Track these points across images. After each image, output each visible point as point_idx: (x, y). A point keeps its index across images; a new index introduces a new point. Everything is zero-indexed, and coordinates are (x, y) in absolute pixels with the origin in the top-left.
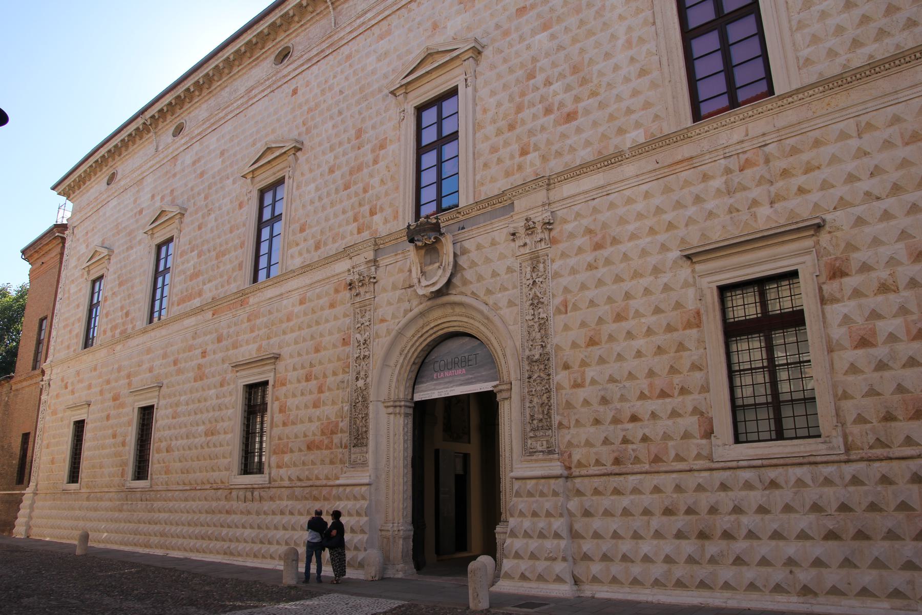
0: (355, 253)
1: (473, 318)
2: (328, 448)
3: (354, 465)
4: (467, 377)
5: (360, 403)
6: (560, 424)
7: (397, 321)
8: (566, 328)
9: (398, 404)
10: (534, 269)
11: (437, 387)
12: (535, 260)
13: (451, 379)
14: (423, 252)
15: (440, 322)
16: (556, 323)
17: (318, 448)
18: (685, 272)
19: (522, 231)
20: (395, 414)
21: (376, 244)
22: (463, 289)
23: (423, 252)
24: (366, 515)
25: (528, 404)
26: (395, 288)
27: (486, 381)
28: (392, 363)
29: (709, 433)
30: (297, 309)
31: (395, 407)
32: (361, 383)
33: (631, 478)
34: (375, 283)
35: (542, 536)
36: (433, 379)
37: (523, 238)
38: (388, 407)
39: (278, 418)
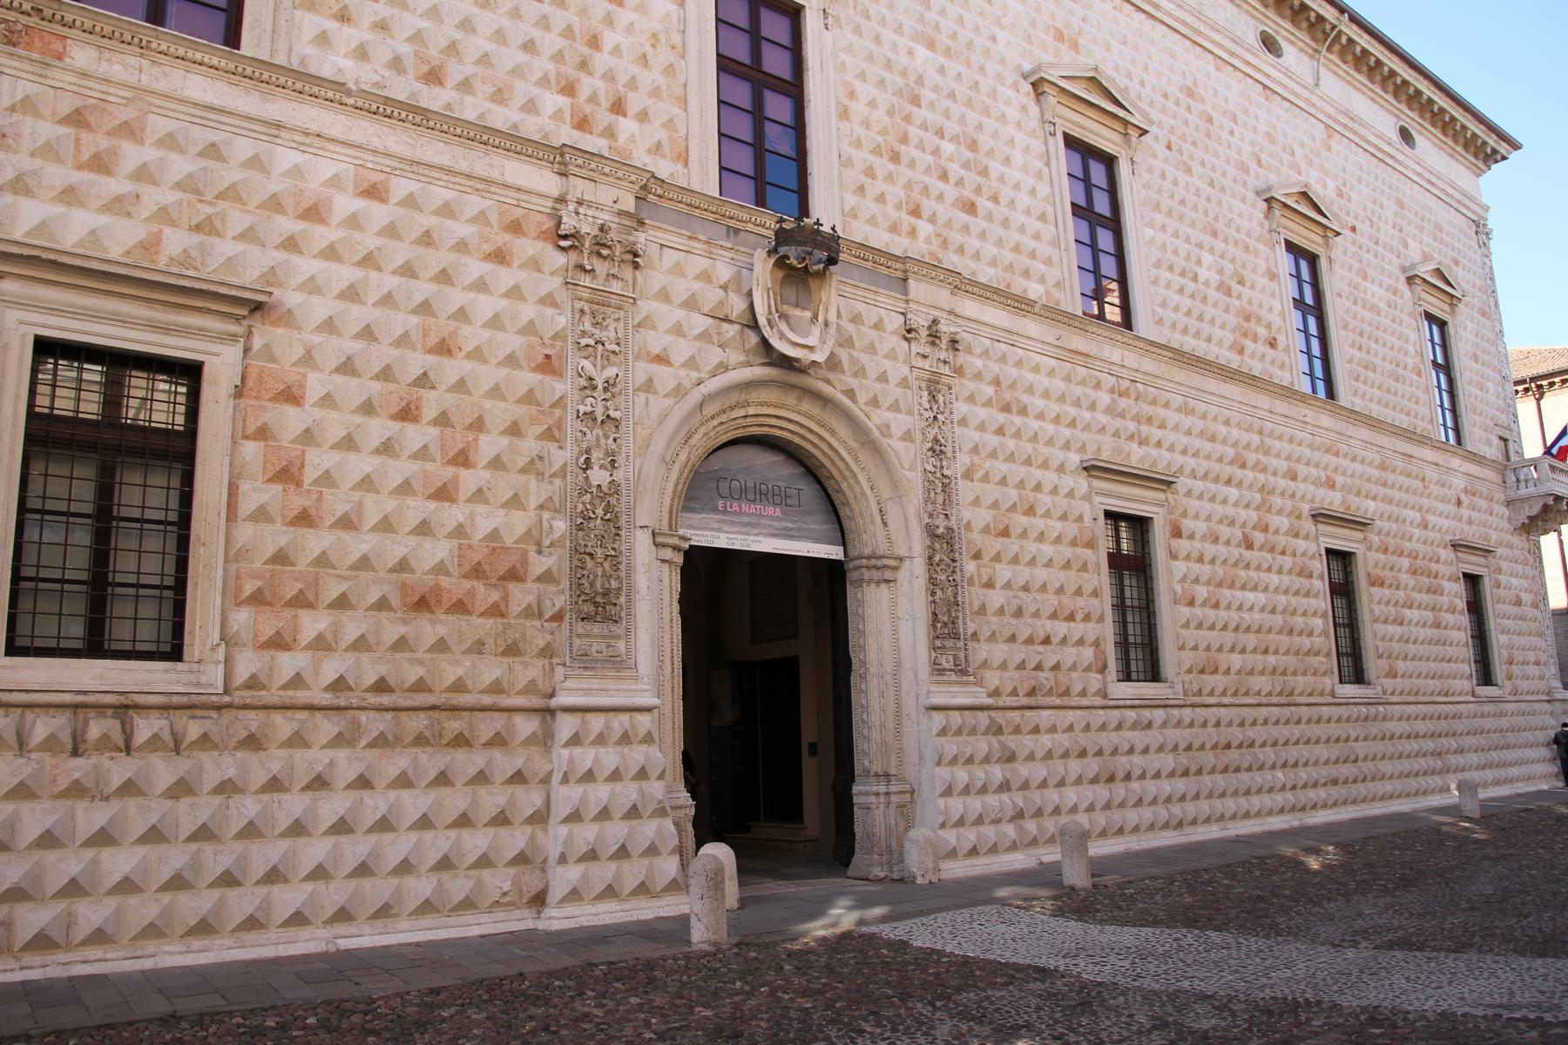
0: (584, 172)
2: (496, 611)
3: (585, 661)
4: (784, 524)
5: (599, 520)
6: (975, 634)
7: (695, 375)
8: (976, 502)
10: (933, 398)
11: (725, 528)
12: (933, 387)
13: (753, 520)
14: (780, 274)
15: (766, 411)
16: (965, 491)
17: (461, 607)
18: (1082, 483)
19: (924, 333)
22: (831, 376)
26: (691, 304)
27: (817, 541)
29: (1103, 669)
30: (345, 204)
32: (599, 476)
33: (1045, 713)
36: (715, 510)
38: (664, 546)
39: (255, 494)
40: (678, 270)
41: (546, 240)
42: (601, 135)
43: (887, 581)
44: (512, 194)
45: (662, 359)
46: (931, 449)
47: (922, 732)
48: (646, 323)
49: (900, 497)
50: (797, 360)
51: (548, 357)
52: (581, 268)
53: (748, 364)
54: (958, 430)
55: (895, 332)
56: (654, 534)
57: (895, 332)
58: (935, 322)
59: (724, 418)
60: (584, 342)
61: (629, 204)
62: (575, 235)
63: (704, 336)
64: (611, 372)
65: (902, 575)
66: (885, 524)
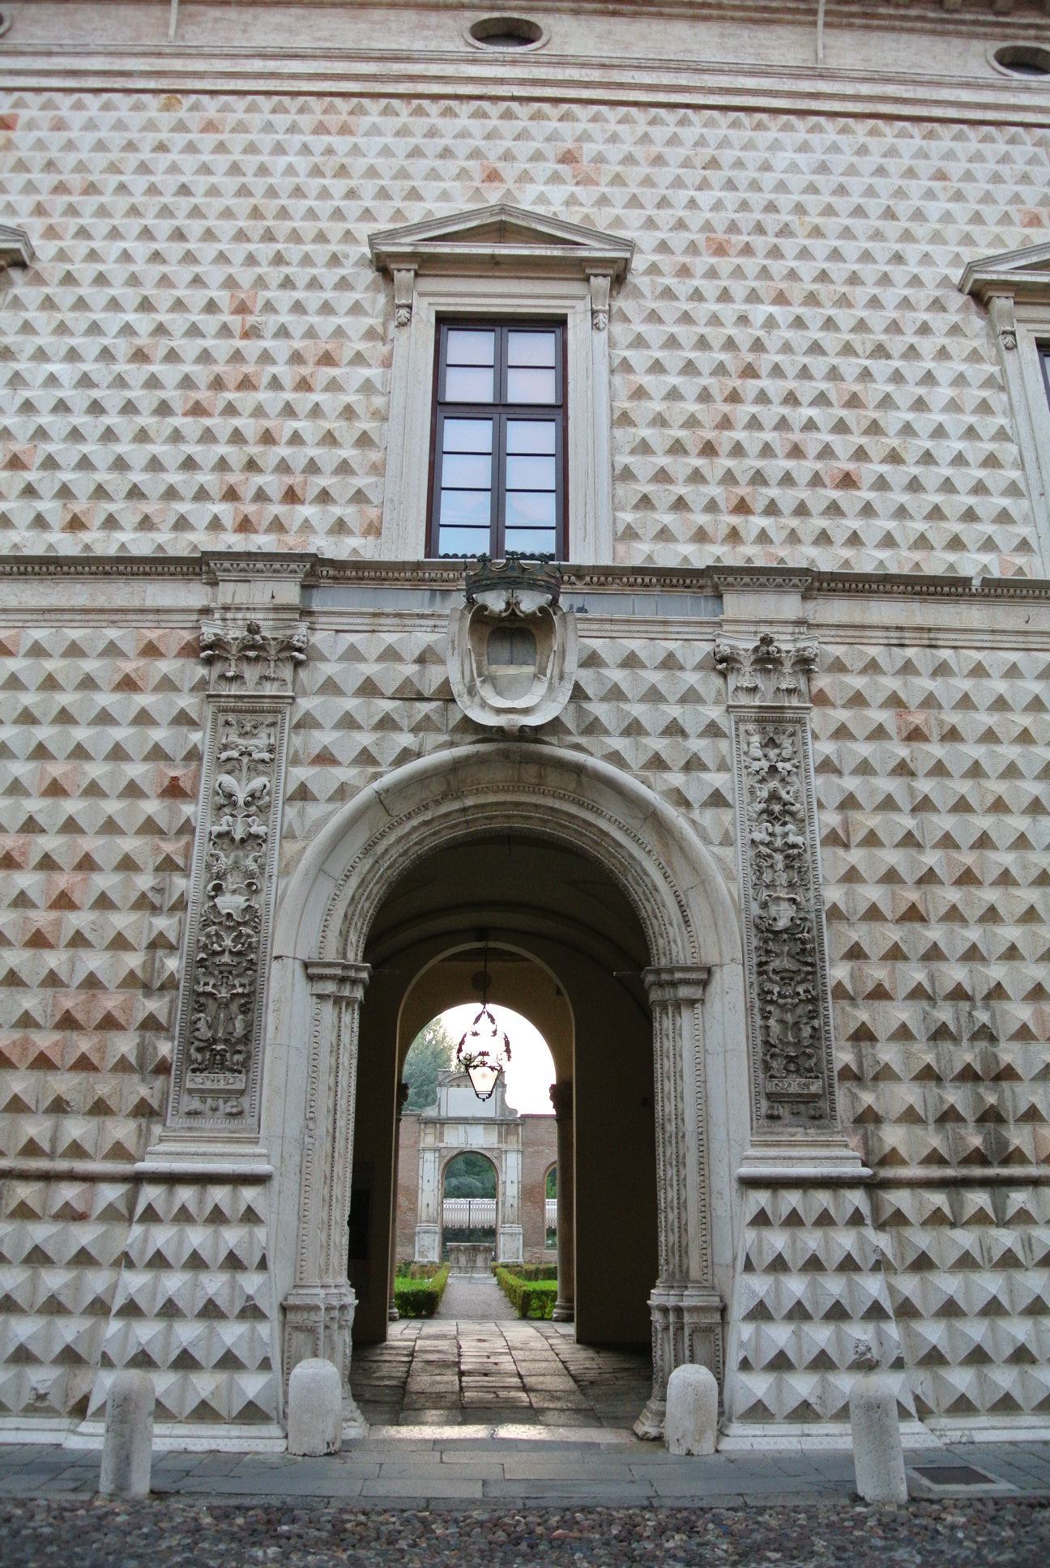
1: (591, 809)
9: (352, 974)
14: (487, 631)
16: (827, 863)
20: (338, 1000)
21: (312, 573)
22: (583, 740)
23: (487, 631)
24: (263, 1265)
25: (759, 1022)
26: (369, 689)
28: (337, 868)
31: (342, 980)
32: (230, 903)
34: (298, 664)
35: (837, 1313)
37: (746, 677)
40: (353, 655)
41: (188, 656)
42: (268, 530)
43: (692, 1003)
44: (151, 617)
45: (325, 758)
46: (768, 812)
47: (733, 1210)
48: (307, 723)
49: (703, 882)
50: (500, 729)
51: (175, 779)
52: (222, 677)
53: (452, 744)
54: (818, 781)
55: (699, 667)
56: (306, 965)
57: (699, 667)
58: (766, 641)
59: (428, 816)
60: (224, 756)
61: (289, 592)
62: (217, 644)
63: (386, 724)
64: (258, 782)
65: (715, 986)
66: (687, 922)
